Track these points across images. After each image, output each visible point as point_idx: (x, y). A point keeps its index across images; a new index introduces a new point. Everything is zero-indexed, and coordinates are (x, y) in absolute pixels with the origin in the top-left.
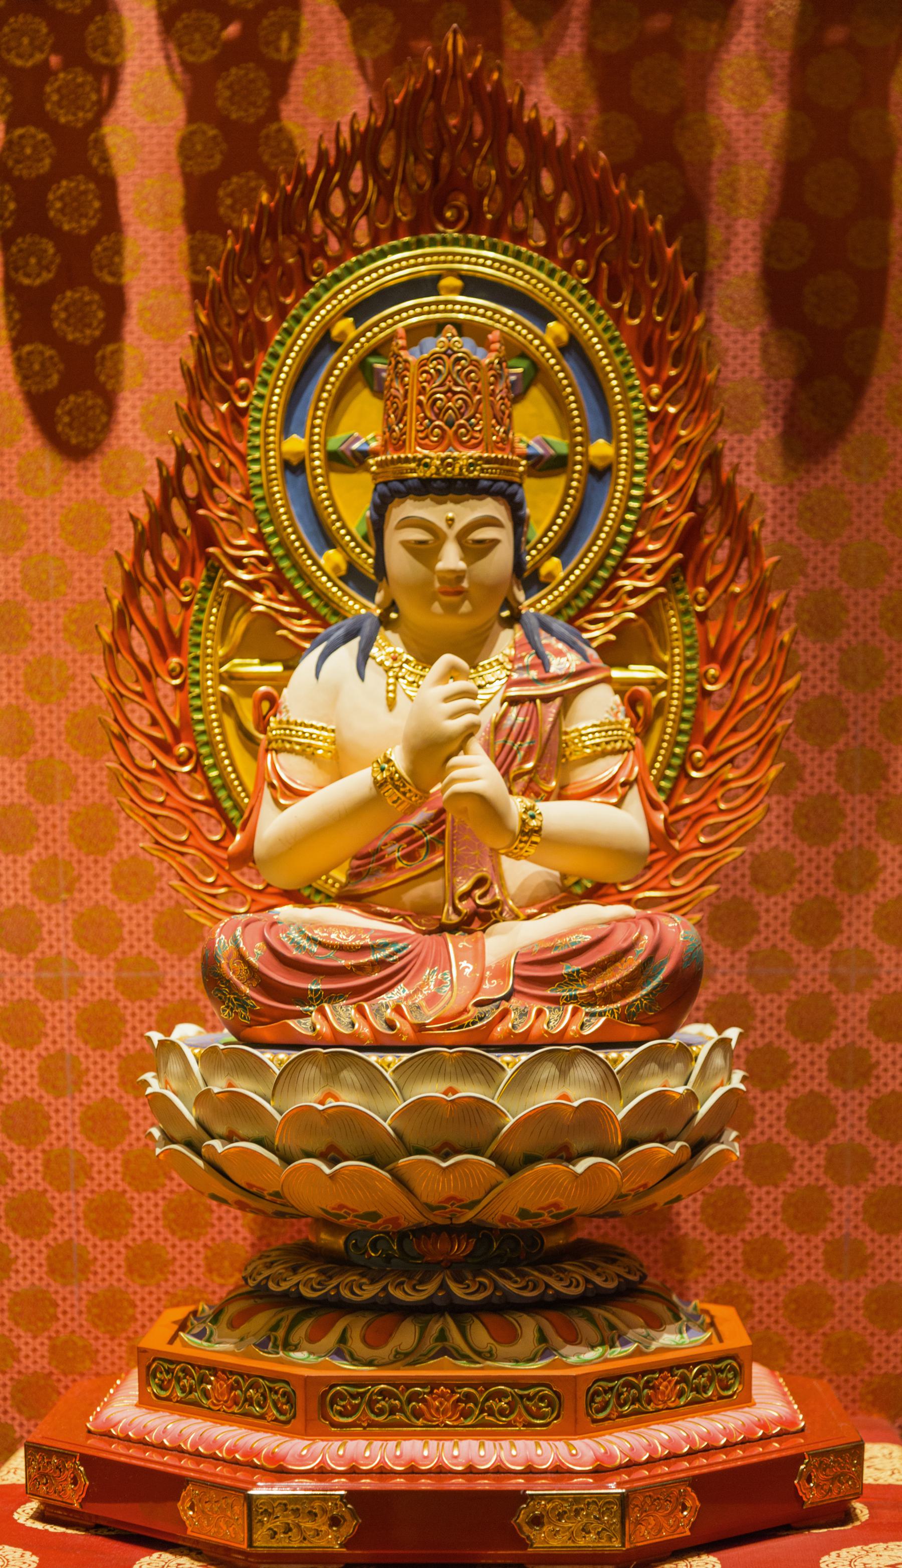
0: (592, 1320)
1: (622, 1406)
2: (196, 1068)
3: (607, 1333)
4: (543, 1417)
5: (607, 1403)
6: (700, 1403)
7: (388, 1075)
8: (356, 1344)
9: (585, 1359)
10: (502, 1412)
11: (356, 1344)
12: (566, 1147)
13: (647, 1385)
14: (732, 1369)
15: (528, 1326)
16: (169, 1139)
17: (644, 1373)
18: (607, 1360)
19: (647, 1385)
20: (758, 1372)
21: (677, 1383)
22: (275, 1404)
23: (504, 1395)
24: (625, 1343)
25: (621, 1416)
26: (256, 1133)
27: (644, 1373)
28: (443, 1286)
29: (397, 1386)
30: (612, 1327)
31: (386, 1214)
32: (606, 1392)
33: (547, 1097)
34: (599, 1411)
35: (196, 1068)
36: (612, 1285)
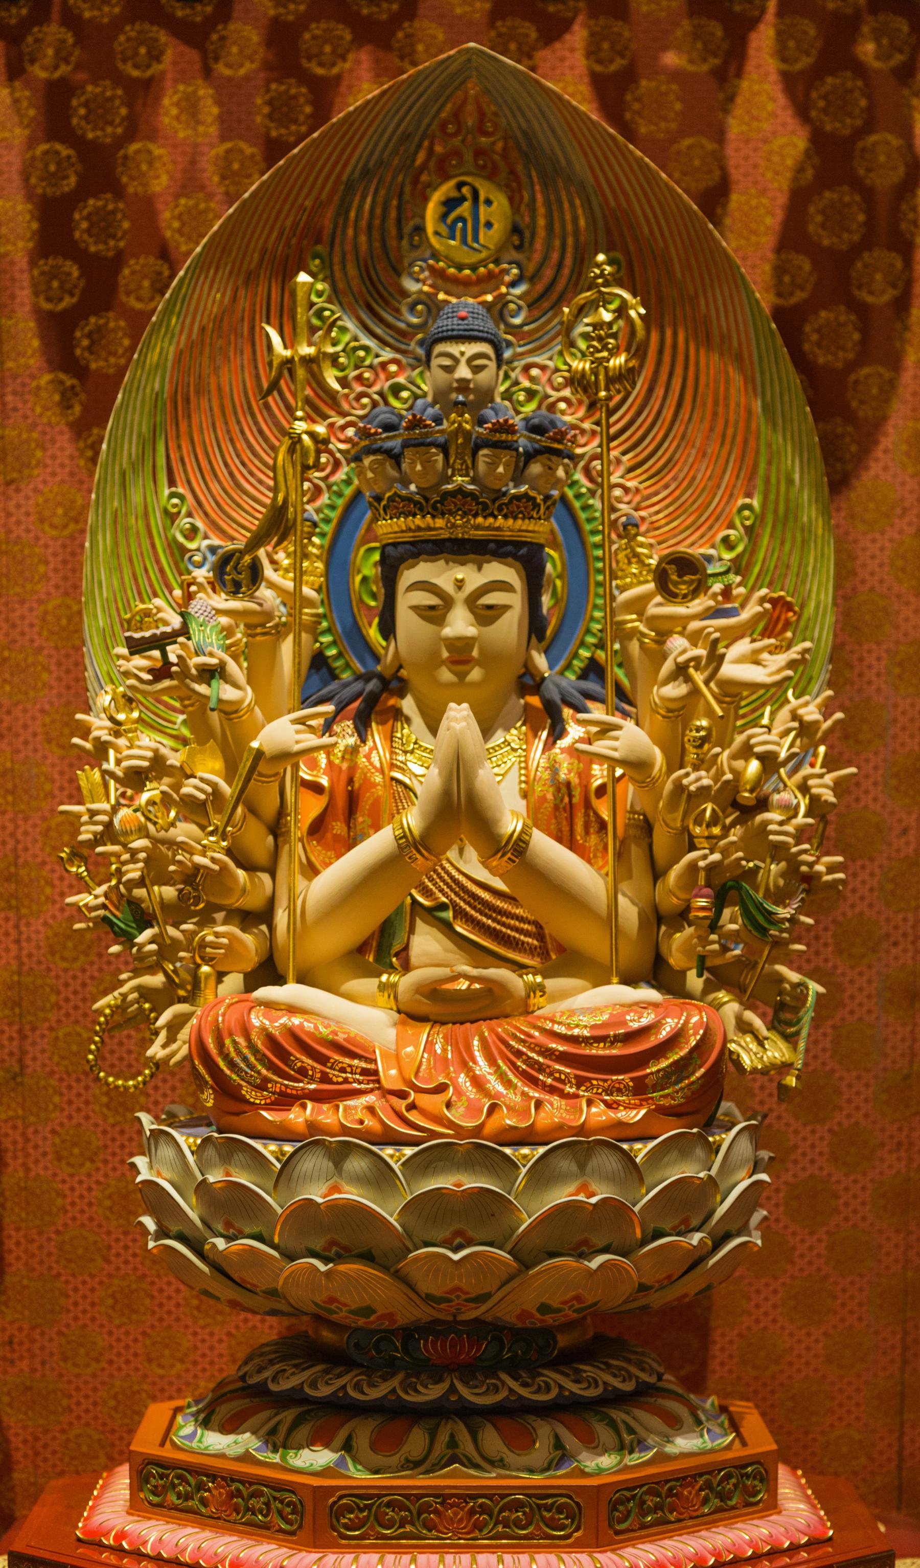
0: (613, 1425)
1: (645, 1515)
2: (191, 1159)
3: (627, 1438)
5: (629, 1512)
7: (396, 1167)
9: (602, 1464)
12: (585, 1242)
13: (670, 1493)
15: (544, 1431)
16: (163, 1233)
18: (627, 1468)
19: (670, 1493)
21: (701, 1489)
24: (647, 1448)
25: (644, 1527)
26: (256, 1229)
27: (667, 1482)
28: (452, 1389)
30: (631, 1431)
35: (191, 1159)
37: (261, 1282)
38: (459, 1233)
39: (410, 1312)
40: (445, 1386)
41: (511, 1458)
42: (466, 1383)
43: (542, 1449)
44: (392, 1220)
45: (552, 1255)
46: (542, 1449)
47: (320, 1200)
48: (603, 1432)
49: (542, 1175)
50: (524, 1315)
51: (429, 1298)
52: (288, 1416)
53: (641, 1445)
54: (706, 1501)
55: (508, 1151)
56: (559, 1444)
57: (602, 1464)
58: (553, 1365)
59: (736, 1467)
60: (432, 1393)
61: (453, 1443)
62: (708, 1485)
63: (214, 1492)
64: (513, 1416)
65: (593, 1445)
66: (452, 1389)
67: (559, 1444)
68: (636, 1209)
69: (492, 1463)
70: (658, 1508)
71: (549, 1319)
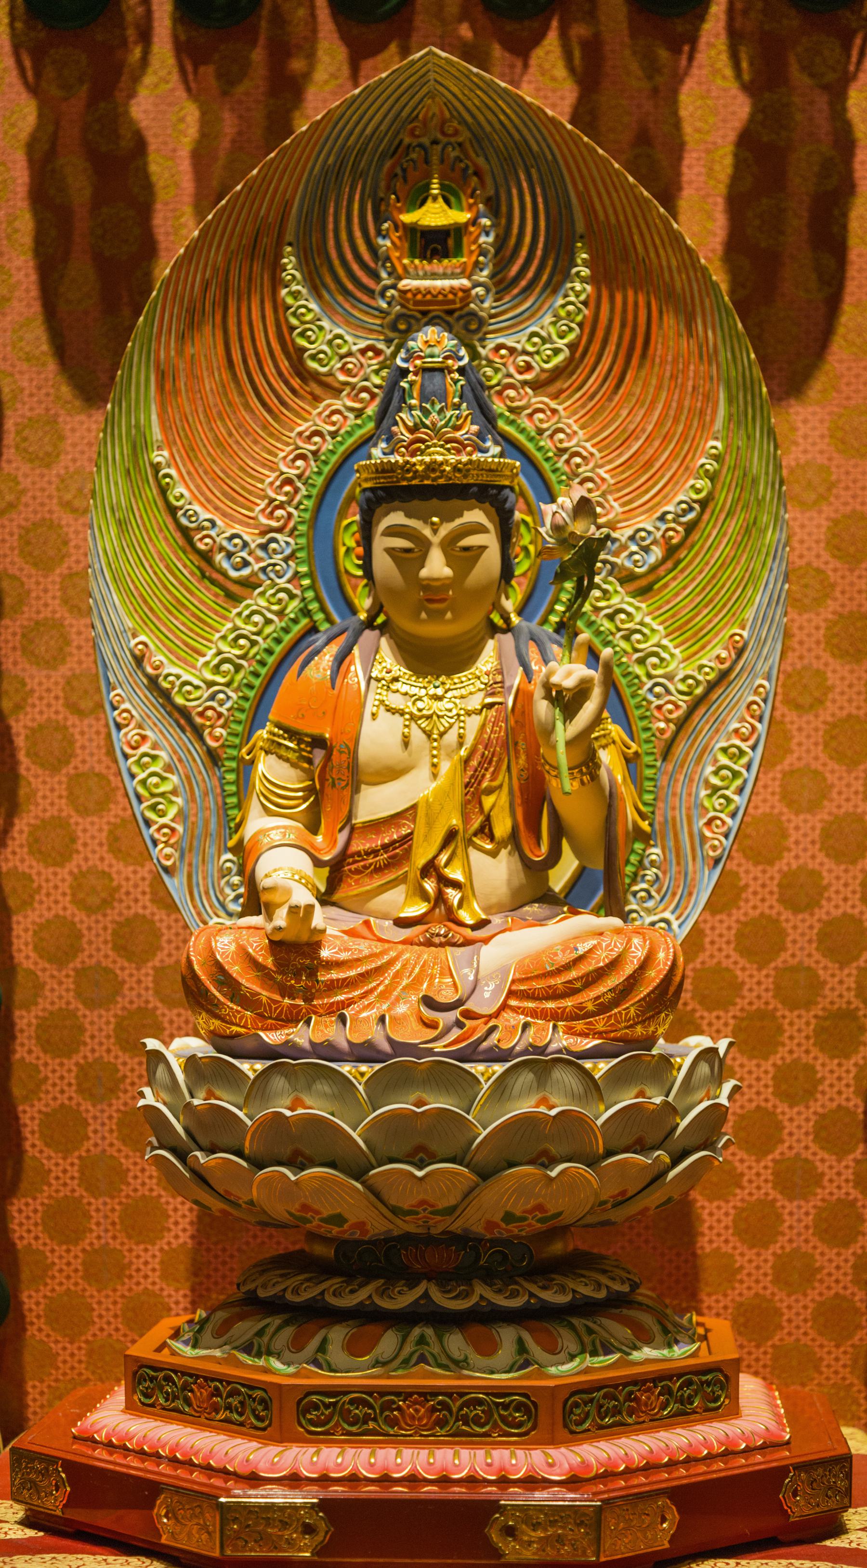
1: (602, 1419)
4: (519, 1425)
8: (336, 1353)
10: (477, 1421)
11: (336, 1353)
13: (628, 1398)
14: (720, 1381)
15: (507, 1335)
17: (625, 1385)
19: (628, 1398)
20: (749, 1386)
22: (253, 1411)
23: (480, 1402)
27: (625, 1385)
29: (370, 1394)
32: (586, 1404)
33: (525, 1106)
34: (580, 1423)
36: (602, 1295)
43: (506, 1352)
45: (511, 1165)
46: (506, 1352)
50: (490, 1225)
56: (522, 1348)
57: (565, 1370)
60: (403, 1299)
63: (199, 1394)
67: (522, 1348)
70: (616, 1411)
71: (514, 1228)
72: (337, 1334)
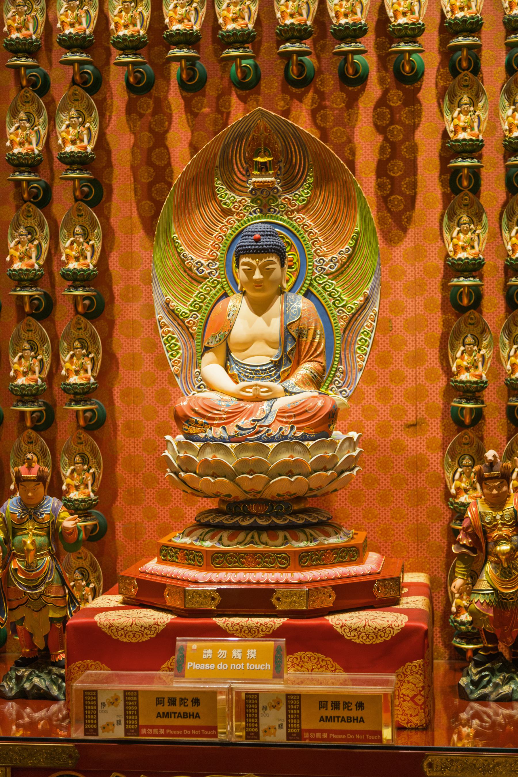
0: (305, 533)
6: (341, 563)
8: (225, 540)
11: (225, 540)
15: (281, 534)
28: (255, 520)
30: (311, 535)
31: (233, 496)
37: (195, 486)
38: (251, 470)
39: (242, 497)
40: (252, 520)
41: (270, 542)
42: (259, 518)
44: (231, 466)
47: (210, 459)
48: (302, 535)
49: (276, 451)
51: (245, 491)
52: (207, 530)
53: (315, 540)
54: (335, 559)
55: (265, 444)
58: (290, 515)
59: (346, 548)
61: (253, 538)
62: (336, 553)
64: (272, 530)
65: (297, 540)
66: (255, 520)
67: (286, 538)
68: (309, 463)
69: (263, 544)
72: (225, 535)
